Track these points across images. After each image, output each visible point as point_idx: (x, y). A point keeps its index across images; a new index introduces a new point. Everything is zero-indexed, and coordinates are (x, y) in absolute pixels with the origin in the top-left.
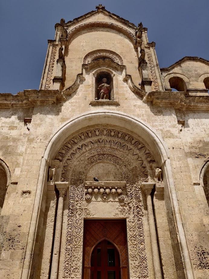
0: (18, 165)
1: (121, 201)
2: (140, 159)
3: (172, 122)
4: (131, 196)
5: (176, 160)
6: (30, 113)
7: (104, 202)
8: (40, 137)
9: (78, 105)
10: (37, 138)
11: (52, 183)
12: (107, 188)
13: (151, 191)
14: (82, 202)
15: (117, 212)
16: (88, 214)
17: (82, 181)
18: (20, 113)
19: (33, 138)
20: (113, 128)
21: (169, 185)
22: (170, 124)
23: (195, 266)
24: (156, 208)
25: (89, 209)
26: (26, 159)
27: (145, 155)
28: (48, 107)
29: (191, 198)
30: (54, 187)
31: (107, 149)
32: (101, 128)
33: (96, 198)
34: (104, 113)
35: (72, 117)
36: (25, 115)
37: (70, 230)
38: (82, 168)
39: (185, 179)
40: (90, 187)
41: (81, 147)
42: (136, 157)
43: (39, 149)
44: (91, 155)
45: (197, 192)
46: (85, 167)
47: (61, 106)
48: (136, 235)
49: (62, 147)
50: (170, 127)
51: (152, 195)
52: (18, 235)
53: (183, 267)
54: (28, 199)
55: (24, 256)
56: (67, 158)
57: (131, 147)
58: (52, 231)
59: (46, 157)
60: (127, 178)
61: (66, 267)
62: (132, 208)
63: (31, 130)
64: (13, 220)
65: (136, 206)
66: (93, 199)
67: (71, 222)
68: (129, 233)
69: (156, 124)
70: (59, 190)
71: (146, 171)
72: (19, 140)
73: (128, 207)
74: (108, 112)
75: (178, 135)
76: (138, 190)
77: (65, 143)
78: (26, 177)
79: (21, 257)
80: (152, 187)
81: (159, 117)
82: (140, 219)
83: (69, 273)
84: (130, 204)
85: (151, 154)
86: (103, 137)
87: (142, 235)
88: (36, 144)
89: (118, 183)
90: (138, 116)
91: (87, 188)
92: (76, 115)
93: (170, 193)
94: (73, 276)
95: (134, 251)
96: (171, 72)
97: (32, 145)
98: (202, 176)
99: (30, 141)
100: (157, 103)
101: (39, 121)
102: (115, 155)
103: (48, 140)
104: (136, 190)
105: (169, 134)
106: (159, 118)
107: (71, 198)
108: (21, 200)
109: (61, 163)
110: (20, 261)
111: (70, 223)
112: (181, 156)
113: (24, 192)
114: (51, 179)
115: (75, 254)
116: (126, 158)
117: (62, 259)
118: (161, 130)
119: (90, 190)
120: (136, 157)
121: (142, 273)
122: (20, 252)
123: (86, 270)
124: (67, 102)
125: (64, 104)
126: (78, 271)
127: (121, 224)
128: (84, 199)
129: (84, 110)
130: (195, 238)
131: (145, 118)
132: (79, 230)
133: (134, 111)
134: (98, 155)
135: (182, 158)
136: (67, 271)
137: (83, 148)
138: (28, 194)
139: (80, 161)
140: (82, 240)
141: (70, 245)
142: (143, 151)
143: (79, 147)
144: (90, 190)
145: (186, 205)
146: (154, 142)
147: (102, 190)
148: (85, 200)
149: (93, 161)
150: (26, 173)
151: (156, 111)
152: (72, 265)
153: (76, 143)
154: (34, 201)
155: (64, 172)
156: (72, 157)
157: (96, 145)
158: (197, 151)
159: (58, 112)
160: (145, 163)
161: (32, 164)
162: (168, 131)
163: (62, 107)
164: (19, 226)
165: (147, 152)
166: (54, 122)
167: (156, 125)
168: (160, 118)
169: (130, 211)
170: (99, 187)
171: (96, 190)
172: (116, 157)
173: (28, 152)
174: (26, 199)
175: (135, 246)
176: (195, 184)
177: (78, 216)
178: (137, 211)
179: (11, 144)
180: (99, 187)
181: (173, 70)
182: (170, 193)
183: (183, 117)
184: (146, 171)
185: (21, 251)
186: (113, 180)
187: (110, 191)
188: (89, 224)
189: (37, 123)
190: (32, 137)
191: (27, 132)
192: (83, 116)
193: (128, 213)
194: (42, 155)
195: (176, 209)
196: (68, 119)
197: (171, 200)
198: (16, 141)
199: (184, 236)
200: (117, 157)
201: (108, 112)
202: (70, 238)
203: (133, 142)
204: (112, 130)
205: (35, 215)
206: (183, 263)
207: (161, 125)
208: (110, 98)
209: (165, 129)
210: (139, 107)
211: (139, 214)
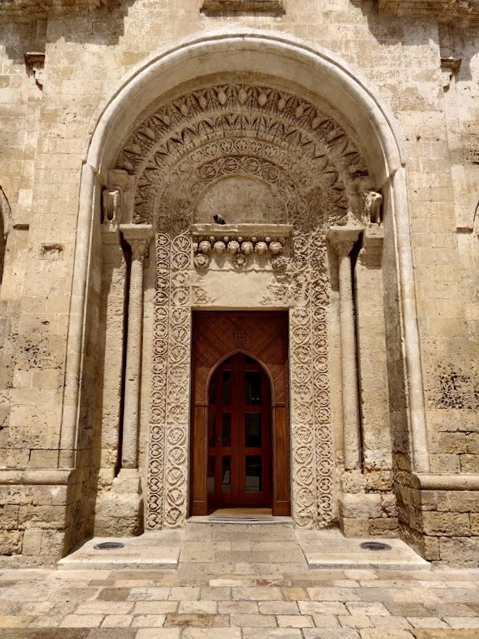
0: (24, 182)
1: (279, 270)
2: (330, 169)
3: (424, 65)
4: (304, 258)
5: (421, 170)
6: (37, 36)
7: (238, 271)
8: (73, 109)
9: (168, 14)
10: (66, 111)
11: (112, 228)
12: (246, 239)
13: (351, 248)
14: (186, 271)
15: (268, 294)
16: (202, 298)
17: (184, 223)
18: (9, 36)
19: (56, 111)
20: (263, 84)
21: (395, 233)
22: (418, 70)
23: (430, 402)
24: (359, 286)
25: (203, 288)
26: (43, 167)
27: (344, 158)
28: (85, 20)
29: (444, 263)
30: (117, 236)
31: (247, 144)
32: (232, 83)
33: (220, 263)
34: (240, 39)
35: (154, 48)
36: (26, 44)
37: (162, 333)
38: (184, 191)
39: (438, 218)
40: (206, 238)
41: (179, 138)
42: (321, 162)
43: (72, 141)
44: (207, 159)
45: (462, 248)
46: (191, 190)
47: (123, 14)
48: (310, 344)
49: (131, 137)
50: (417, 78)
51: (353, 256)
52: (45, 341)
53: (405, 404)
54: (59, 262)
55: (63, 382)
56: (145, 164)
58: (120, 334)
59: (92, 161)
60: (295, 215)
61: (156, 403)
62: (304, 286)
63: (48, 87)
64: (29, 310)
65: (313, 281)
66: (213, 265)
67: (164, 316)
68: (294, 340)
69: (382, 69)
70: (130, 242)
71: (343, 199)
72: (18, 115)
73: (293, 285)
74: (253, 36)
75: (437, 101)
76: (319, 244)
77: (138, 124)
78: (49, 212)
79: (56, 384)
80: (356, 238)
81: (392, 48)
82: (321, 311)
83: (163, 414)
84: (298, 278)
85: (359, 155)
86: (238, 110)
87: (322, 343)
88: (65, 126)
89: (272, 228)
90: (335, 46)
91: (198, 239)
92: (164, 44)
93: (396, 251)
94: (170, 420)
95: (302, 375)
97: (55, 131)
99: (49, 118)
101: (64, 63)
102: (269, 159)
103: (95, 116)
104: (315, 245)
105: (412, 100)
106: (390, 52)
107: (161, 263)
108: (42, 266)
109: (133, 177)
110: (55, 391)
111: (161, 317)
112: (436, 158)
113: (47, 249)
114: (110, 218)
115: (173, 379)
116: (295, 167)
117: (146, 388)
118: (393, 88)
119: (205, 245)
120: (321, 162)
121: (317, 416)
122: (52, 375)
123: (199, 411)
125: (131, 10)
126: (181, 412)
127: (277, 321)
128: (192, 266)
129: (186, 30)
130: (441, 349)
131: (353, 51)
132: (182, 332)
133: (324, 31)
134: (225, 157)
135: (437, 165)
136: (157, 412)
137: (185, 139)
138: (57, 251)
139: (180, 173)
140: (188, 353)
141: (162, 362)
142: (341, 148)
143: (175, 137)
144: (205, 245)
145: (432, 278)
146: (370, 121)
147: (233, 245)
148: (194, 267)
149: (212, 174)
150: (46, 201)
151: (385, 31)
152: (168, 401)
153: (167, 126)
154: (74, 266)
155: (140, 200)
156: (159, 163)
157: (219, 132)
159: (114, 34)
160: (343, 177)
161: (60, 179)
162: (411, 91)
163: (125, 18)
164: (45, 323)
165: (350, 149)
166: (105, 65)
167: (381, 73)
168: (395, 50)
169: (299, 292)
170: (226, 238)
171: (219, 245)
172: (271, 163)
173: (45, 149)
174: (54, 264)
175: (306, 366)
176: (460, 230)
177: (178, 303)
178: (314, 292)
180: (226, 238)
182: (396, 251)
183: (458, 49)
184: (343, 199)
185: (57, 372)
186: (260, 222)
187: (254, 247)
188: (204, 321)
189: (61, 66)
190: (51, 107)
191: (37, 93)
192: (183, 46)
193: (293, 298)
194: (83, 157)
195: (407, 289)
196: (142, 55)
197: (398, 267)
198: (12, 118)
199: (417, 346)
200: (274, 164)
201: (253, 36)
202: (162, 349)
203: (316, 122)
204: (262, 88)
205: (77, 298)
206: (407, 398)
207: (392, 74)
209: (404, 86)
210: (340, 18)
211: (319, 299)
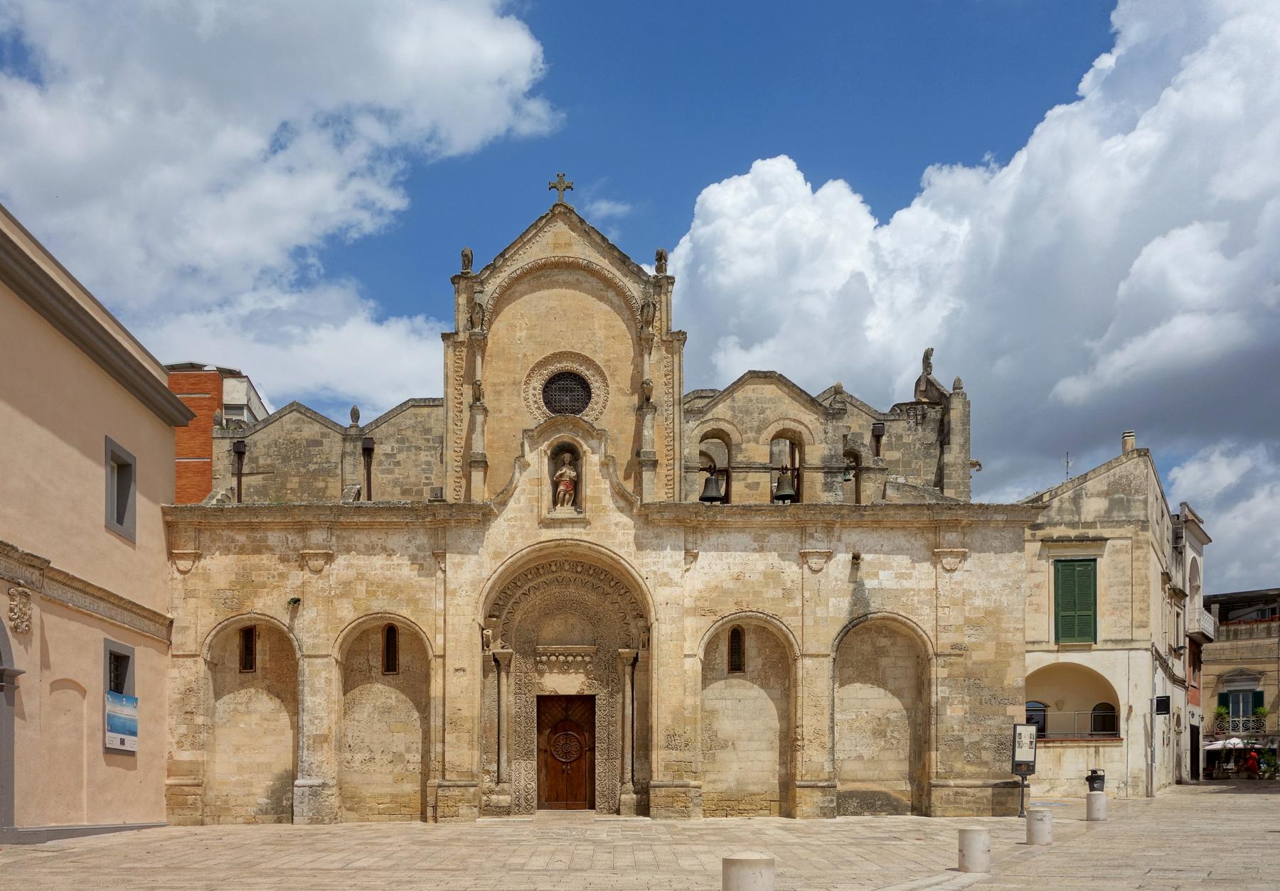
22: (670, 561)
45: (687, 667)
50: (669, 565)
57: (610, 591)
96: (709, 416)
98: (703, 645)
100: (654, 521)
124: (500, 520)
130: (669, 722)
158: (707, 604)
162: (665, 574)
179: (421, 595)
181: (714, 410)
196: (505, 554)
207: (654, 563)
208: (576, 503)
210: (624, 527)
